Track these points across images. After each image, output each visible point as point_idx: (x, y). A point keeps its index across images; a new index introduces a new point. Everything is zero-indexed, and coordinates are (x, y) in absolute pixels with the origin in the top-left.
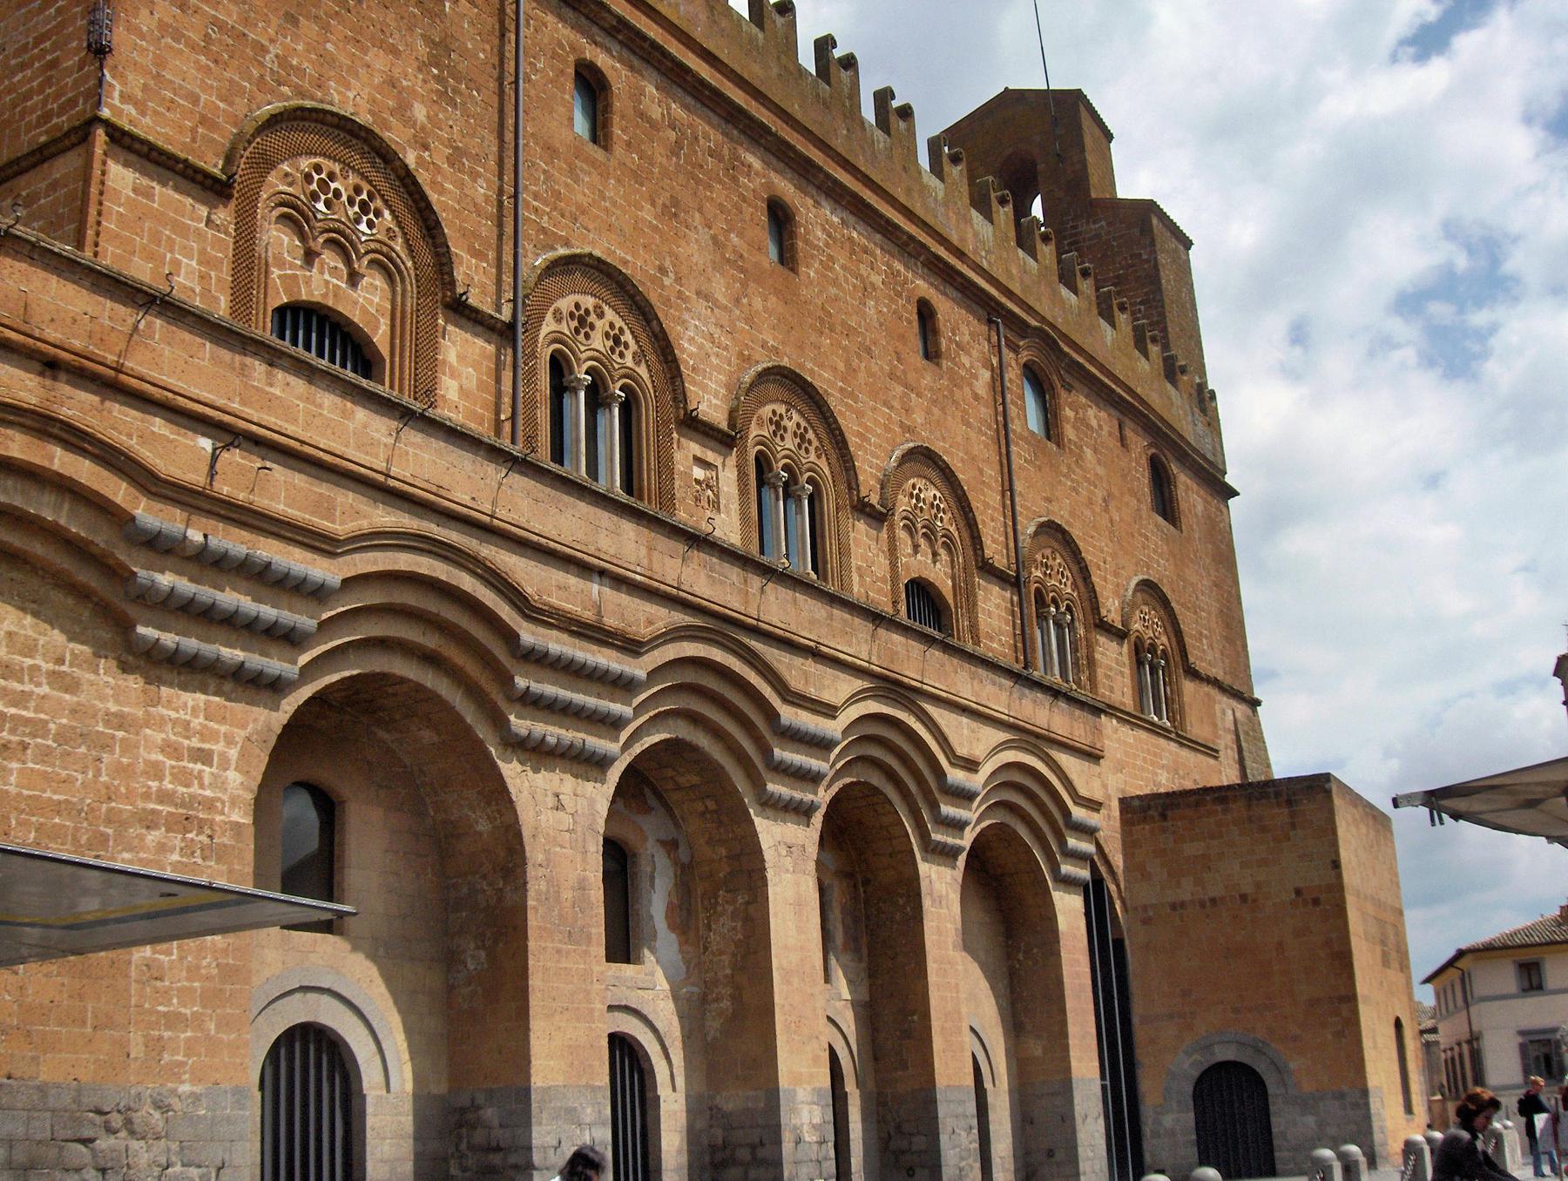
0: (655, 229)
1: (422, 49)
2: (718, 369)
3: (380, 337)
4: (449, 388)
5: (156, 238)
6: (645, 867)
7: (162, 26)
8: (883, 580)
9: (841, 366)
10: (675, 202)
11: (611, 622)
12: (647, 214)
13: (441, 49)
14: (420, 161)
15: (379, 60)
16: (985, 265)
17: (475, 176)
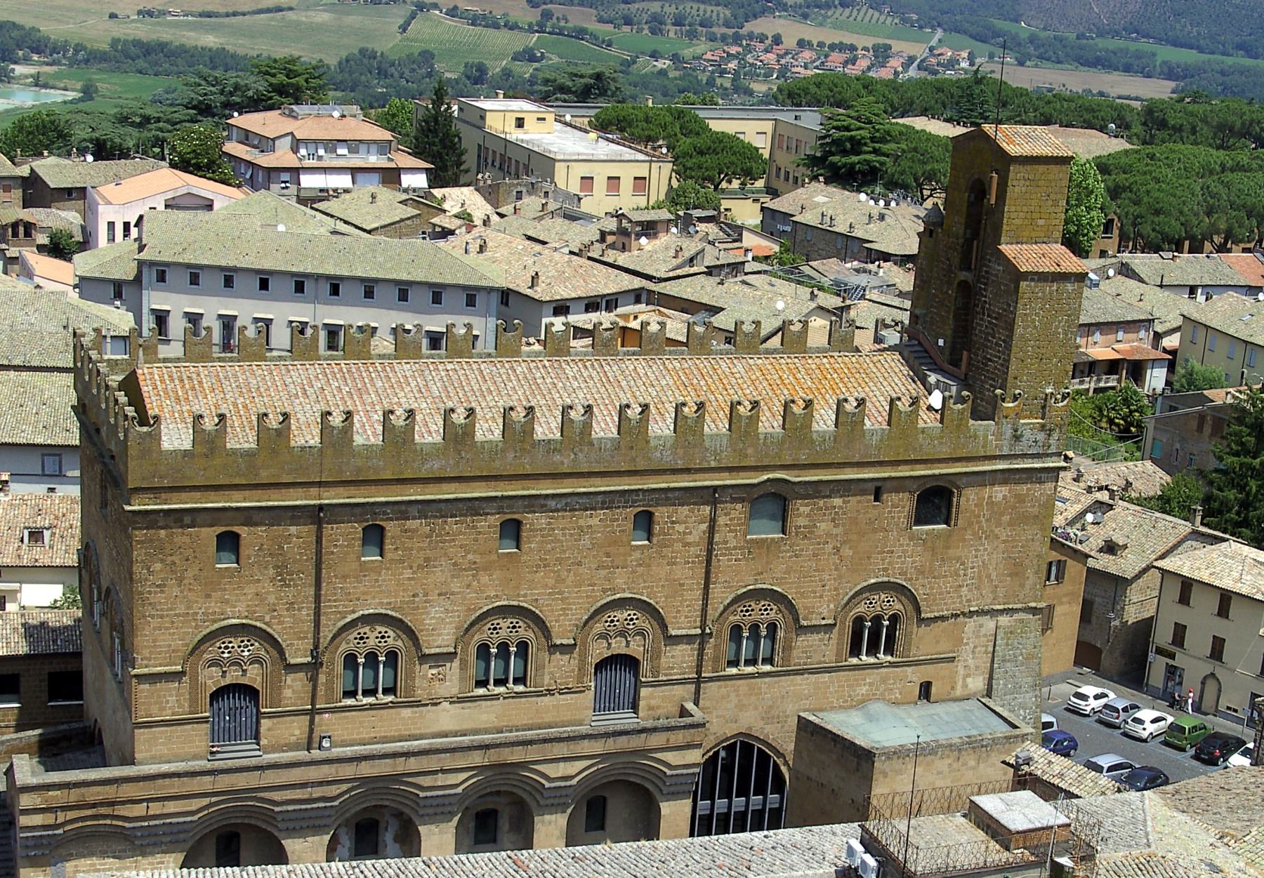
0: (412, 579)
1: (271, 571)
2: (450, 623)
3: (257, 686)
4: (288, 693)
5: (159, 697)
6: (382, 825)
7: (154, 629)
8: (573, 671)
9: (551, 582)
10: (427, 560)
11: (314, 796)
12: (408, 573)
13: (281, 569)
14: (273, 617)
15: (250, 590)
16: (713, 464)
17: (299, 610)
